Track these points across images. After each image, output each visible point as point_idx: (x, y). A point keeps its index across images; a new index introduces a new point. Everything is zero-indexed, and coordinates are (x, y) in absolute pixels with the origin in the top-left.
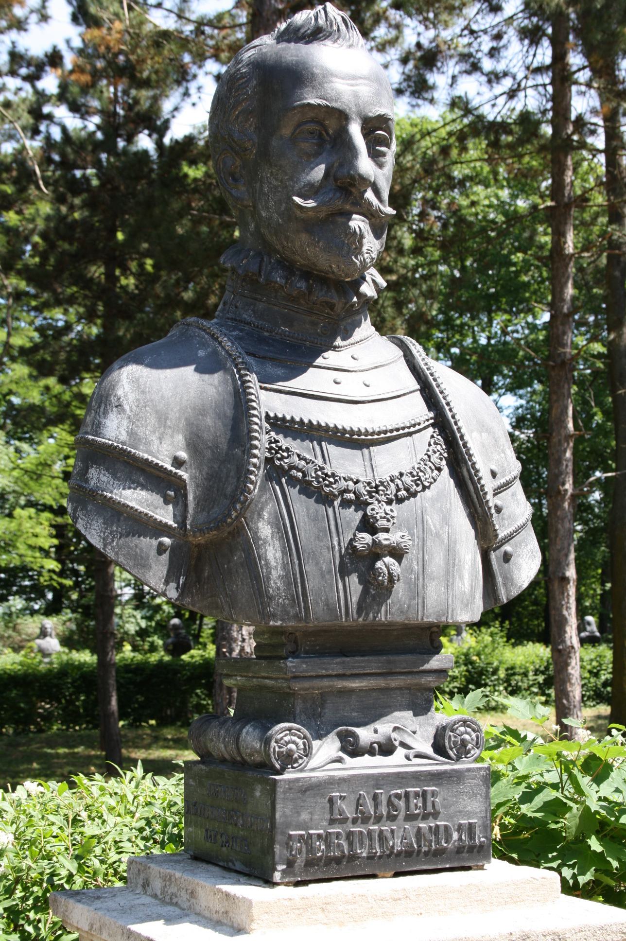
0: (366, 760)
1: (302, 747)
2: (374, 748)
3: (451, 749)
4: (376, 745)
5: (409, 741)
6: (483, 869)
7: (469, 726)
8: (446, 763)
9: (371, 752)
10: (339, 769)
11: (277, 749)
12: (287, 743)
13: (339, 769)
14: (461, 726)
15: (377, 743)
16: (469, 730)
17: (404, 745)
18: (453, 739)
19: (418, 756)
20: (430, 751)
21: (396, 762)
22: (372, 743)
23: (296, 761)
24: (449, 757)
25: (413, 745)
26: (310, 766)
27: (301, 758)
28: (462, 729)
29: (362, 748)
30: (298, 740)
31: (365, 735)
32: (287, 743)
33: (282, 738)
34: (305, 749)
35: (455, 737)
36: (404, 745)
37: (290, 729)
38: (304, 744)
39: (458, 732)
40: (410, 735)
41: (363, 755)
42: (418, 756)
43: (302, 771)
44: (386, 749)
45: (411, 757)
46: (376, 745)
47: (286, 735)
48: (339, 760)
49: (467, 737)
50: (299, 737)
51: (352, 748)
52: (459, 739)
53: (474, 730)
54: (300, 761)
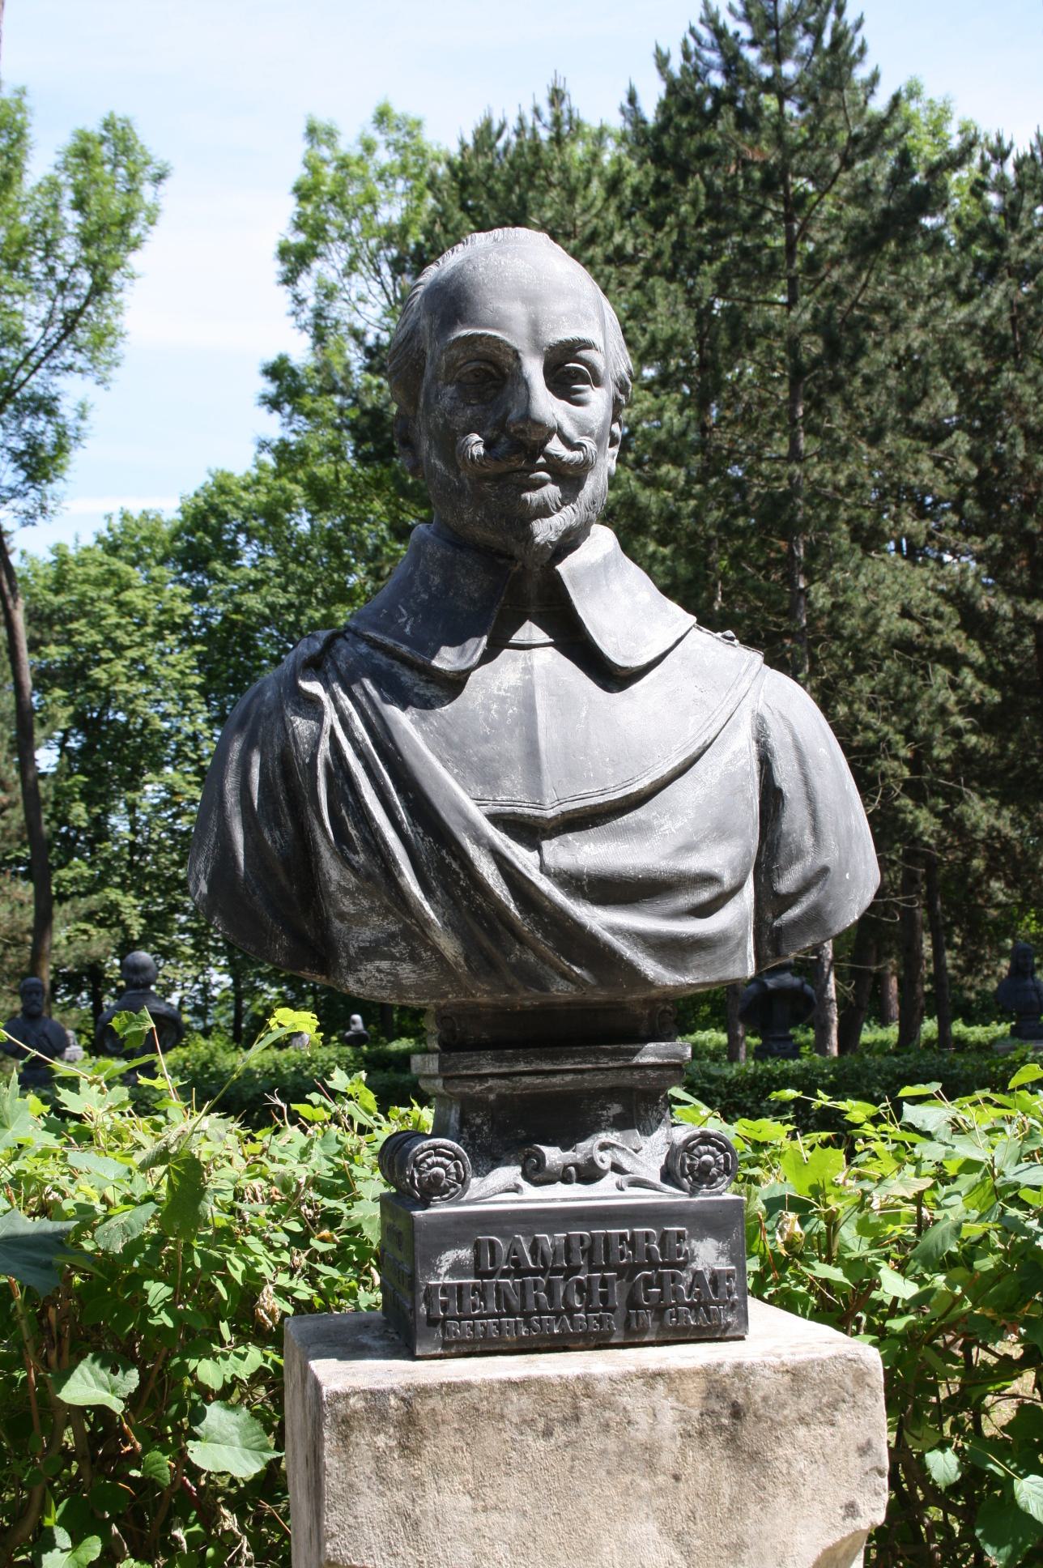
1: (453, 1170)
2: (570, 1174)
4: (572, 1169)
5: (626, 1163)
7: (713, 1144)
9: (566, 1179)
10: (513, 1202)
11: (416, 1175)
13: (513, 1202)
14: (700, 1143)
15: (576, 1165)
17: (617, 1168)
19: (637, 1183)
20: (656, 1179)
21: (605, 1192)
22: (566, 1167)
23: (445, 1190)
24: (680, 1187)
28: (702, 1148)
29: (550, 1172)
30: (447, 1162)
31: (553, 1155)
33: (423, 1161)
34: (458, 1175)
36: (617, 1168)
37: (434, 1148)
38: (456, 1166)
40: (629, 1154)
42: (637, 1183)
44: (588, 1174)
46: (572, 1169)
47: (429, 1156)
48: (517, 1189)
49: (708, 1158)
51: (538, 1174)
53: (721, 1149)
54: (452, 1190)
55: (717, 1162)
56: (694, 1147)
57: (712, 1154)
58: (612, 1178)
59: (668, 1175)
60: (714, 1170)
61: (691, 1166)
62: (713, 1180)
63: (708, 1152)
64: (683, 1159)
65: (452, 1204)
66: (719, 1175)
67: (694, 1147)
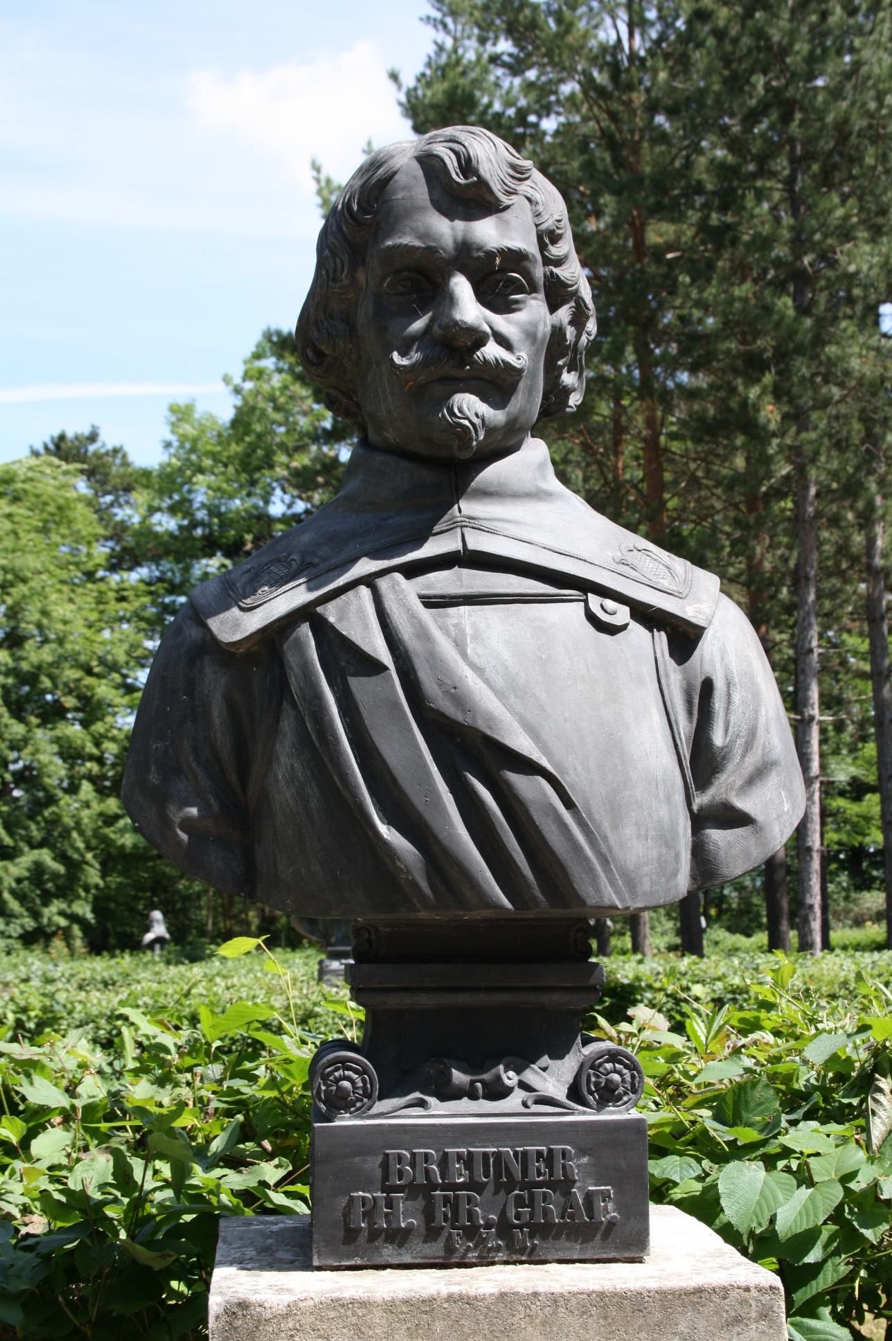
0: (465, 1104)
1: (360, 1084)
3: (591, 1093)
6: (641, 1262)
7: (621, 1062)
8: (584, 1113)
9: (473, 1096)
11: (323, 1088)
12: (338, 1080)
14: (607, 1061)
16: (618, 1066)
17: (524, 1086)
18: (593, 1079)
20: (560, 1093)
25: (536, 1087)
26: (374, 1111)
27: (361, 1100)
28: (609, 1066)
30: (355, 1076)
32: (338, 1080)
33: (332, 1073)
34: (364, 1088)
35: (598, 1076)
36: (524, 1086)
38: (364, 1081)
39: (601, 1069)
41: (460, 1098)
43: (363, 1118)
44: (497, 1092)
45: (529, 1103)
46: (479, 1085)
47: (337, 1069)
49: (616, 1077)
50: (356, 1071)
52: (603, 1080)
53: (626, 1067)
54: (358, 1104)
55: (623, 1081)
56: (601, 1065)
57: (619, 1073)
58: (518, 1096)
59: (575, 1093)
60: (621, 1090)
61: (597, 1084)
62: (619, 1098)
63: (615, 1071)
64: (589, 1076)
65: (357, 1117)
66: (626, 1093)
67: (601, 1065)
